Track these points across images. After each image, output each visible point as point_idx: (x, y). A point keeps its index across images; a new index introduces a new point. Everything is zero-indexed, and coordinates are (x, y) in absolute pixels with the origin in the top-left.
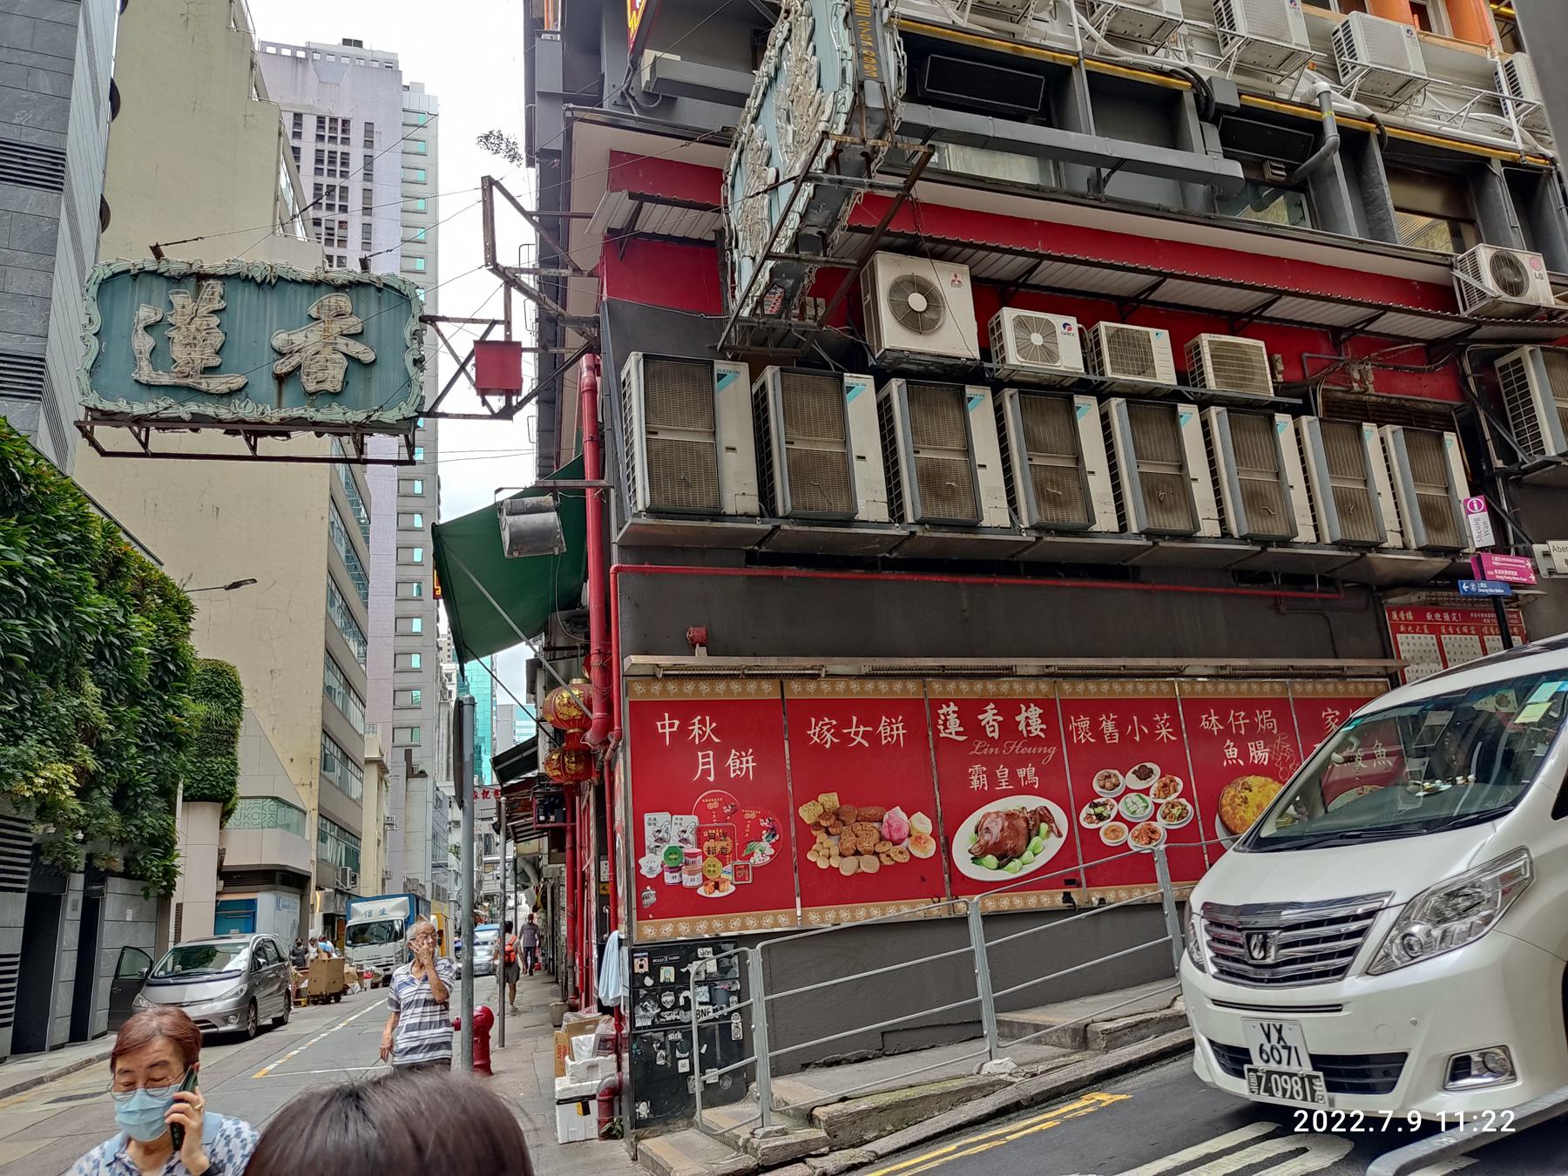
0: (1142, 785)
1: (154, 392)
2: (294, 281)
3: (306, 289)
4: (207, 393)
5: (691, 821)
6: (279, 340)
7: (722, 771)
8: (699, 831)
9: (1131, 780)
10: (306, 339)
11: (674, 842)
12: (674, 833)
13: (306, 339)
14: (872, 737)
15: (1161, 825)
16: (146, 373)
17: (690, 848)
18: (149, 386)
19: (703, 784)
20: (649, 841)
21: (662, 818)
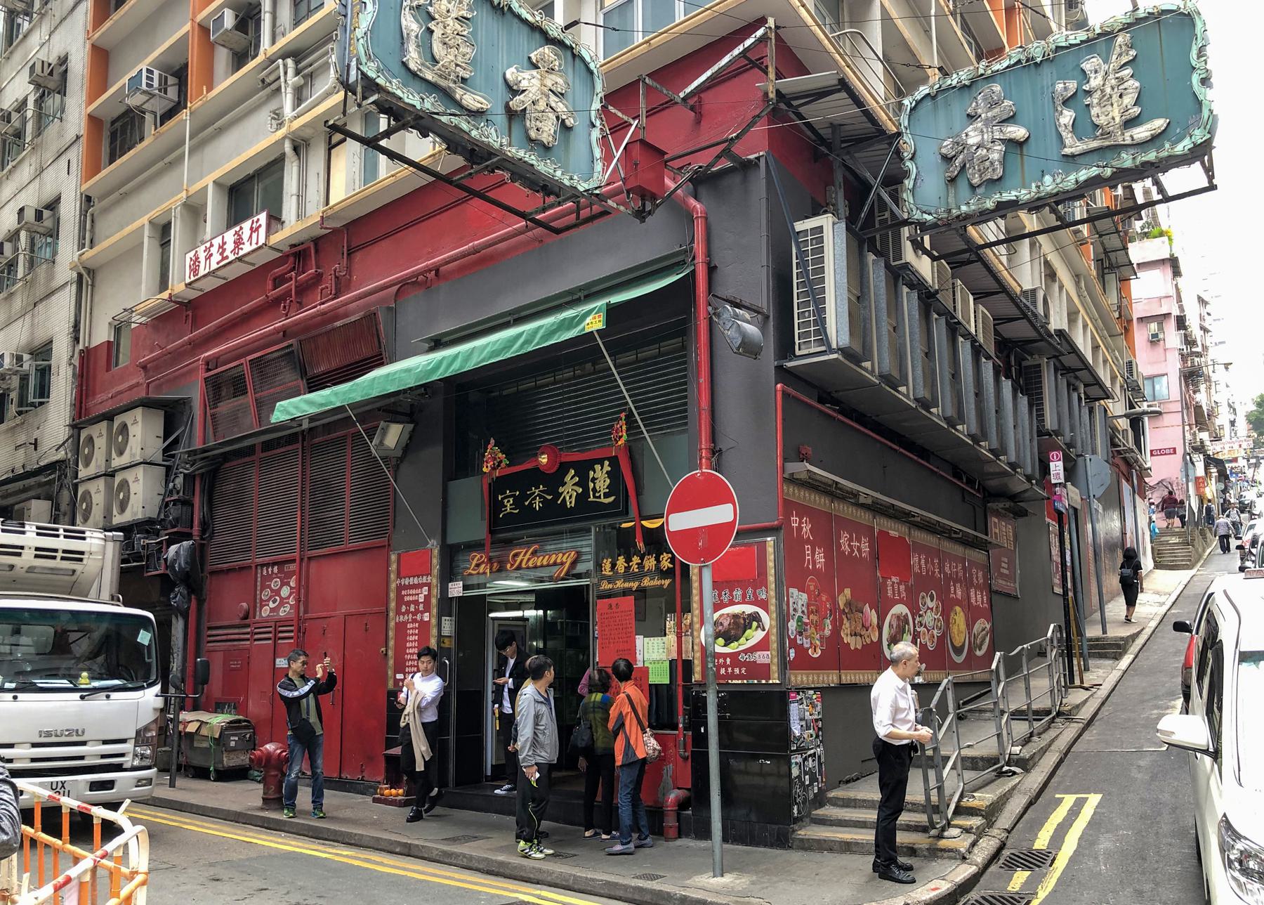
0: (931, 604)
1: (418, 83)
2: (519, 17)
3: (525, 30)
4: (459, 105)
5: (805, 596)
6: (511, 74)
7: (814, 563)
8: (808, 605)
9: (928, 600)
10: (530, 82)
11: (799, 614)
12: (800, 603)
13: (530, 82)
14: (859, 549)
15: (935, 632)
16: (414, 58)
17: (806, 620)
18: (414, 75)
19: (809, 572)
20: (792, 612)
21: (794, 591)
